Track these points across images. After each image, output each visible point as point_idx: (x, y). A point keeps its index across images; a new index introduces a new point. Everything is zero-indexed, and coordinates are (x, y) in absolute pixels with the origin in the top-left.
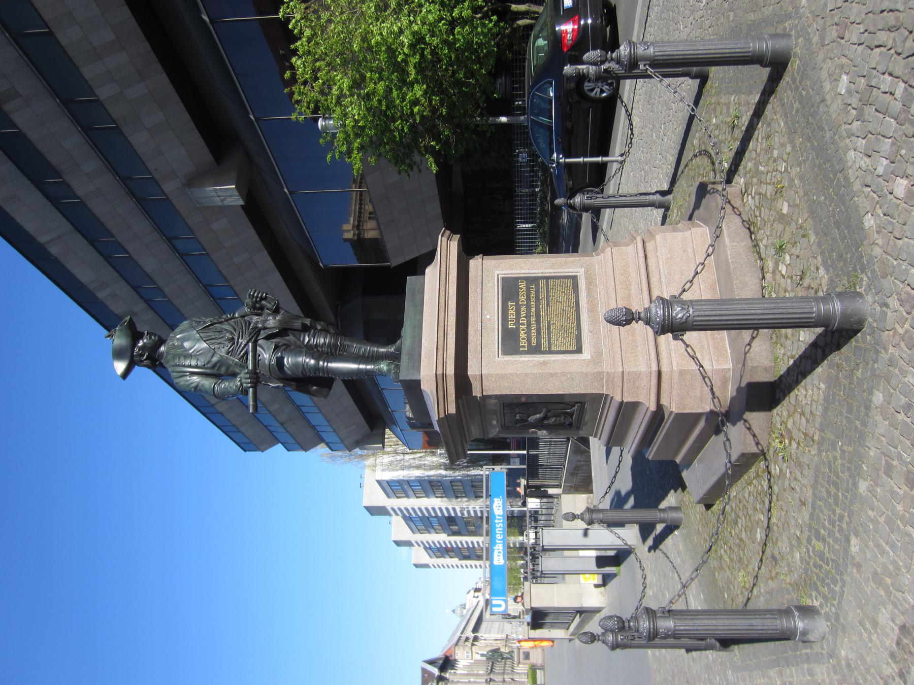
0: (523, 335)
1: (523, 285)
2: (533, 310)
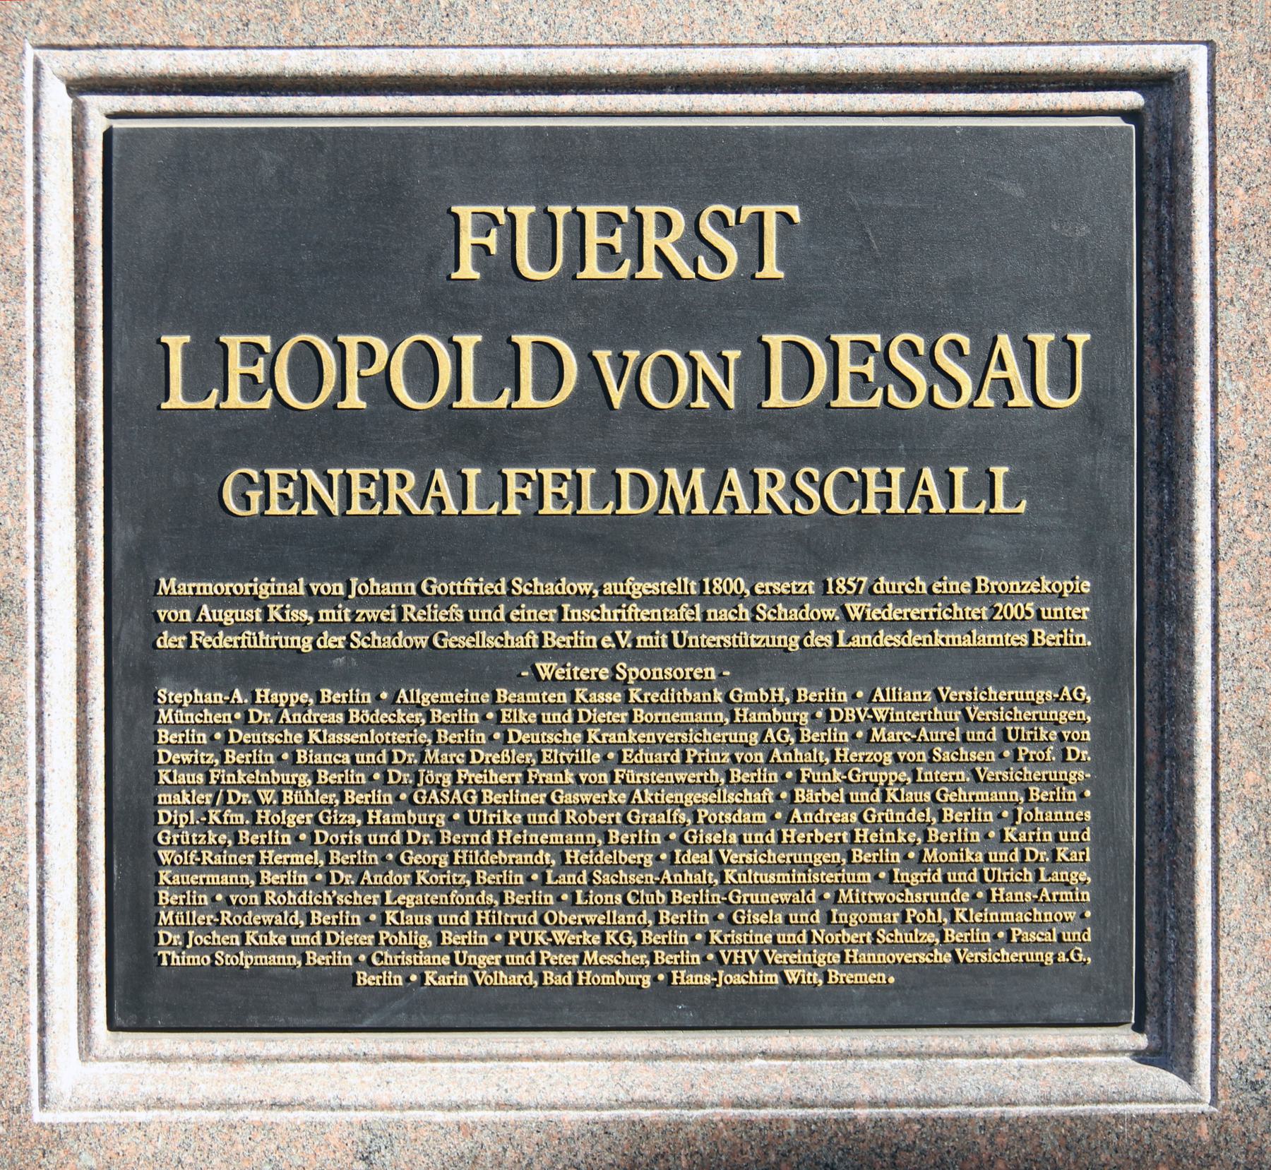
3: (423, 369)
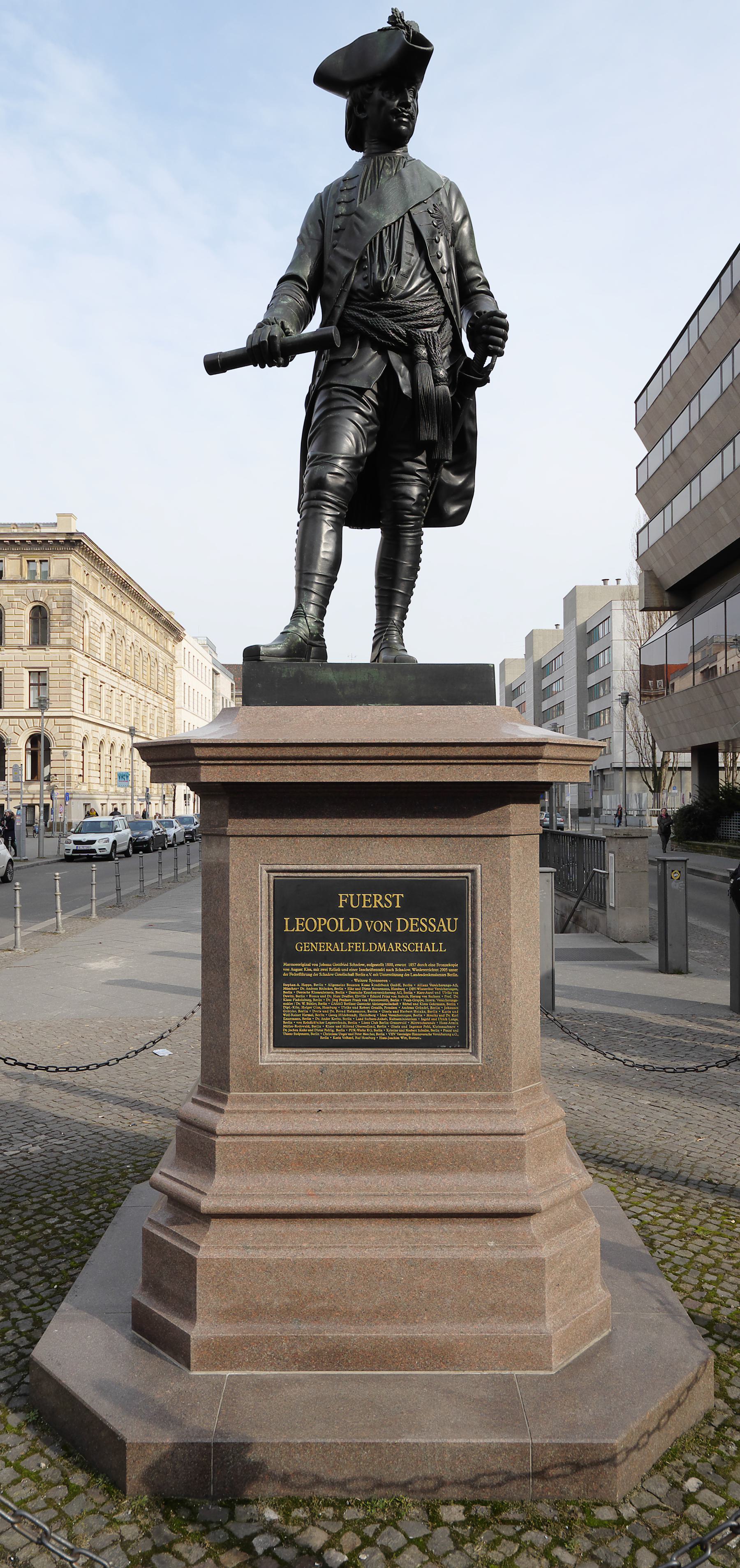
0: (320, 923)
1: (446, 926)
2: (382, 947)
3: (333, 924)
